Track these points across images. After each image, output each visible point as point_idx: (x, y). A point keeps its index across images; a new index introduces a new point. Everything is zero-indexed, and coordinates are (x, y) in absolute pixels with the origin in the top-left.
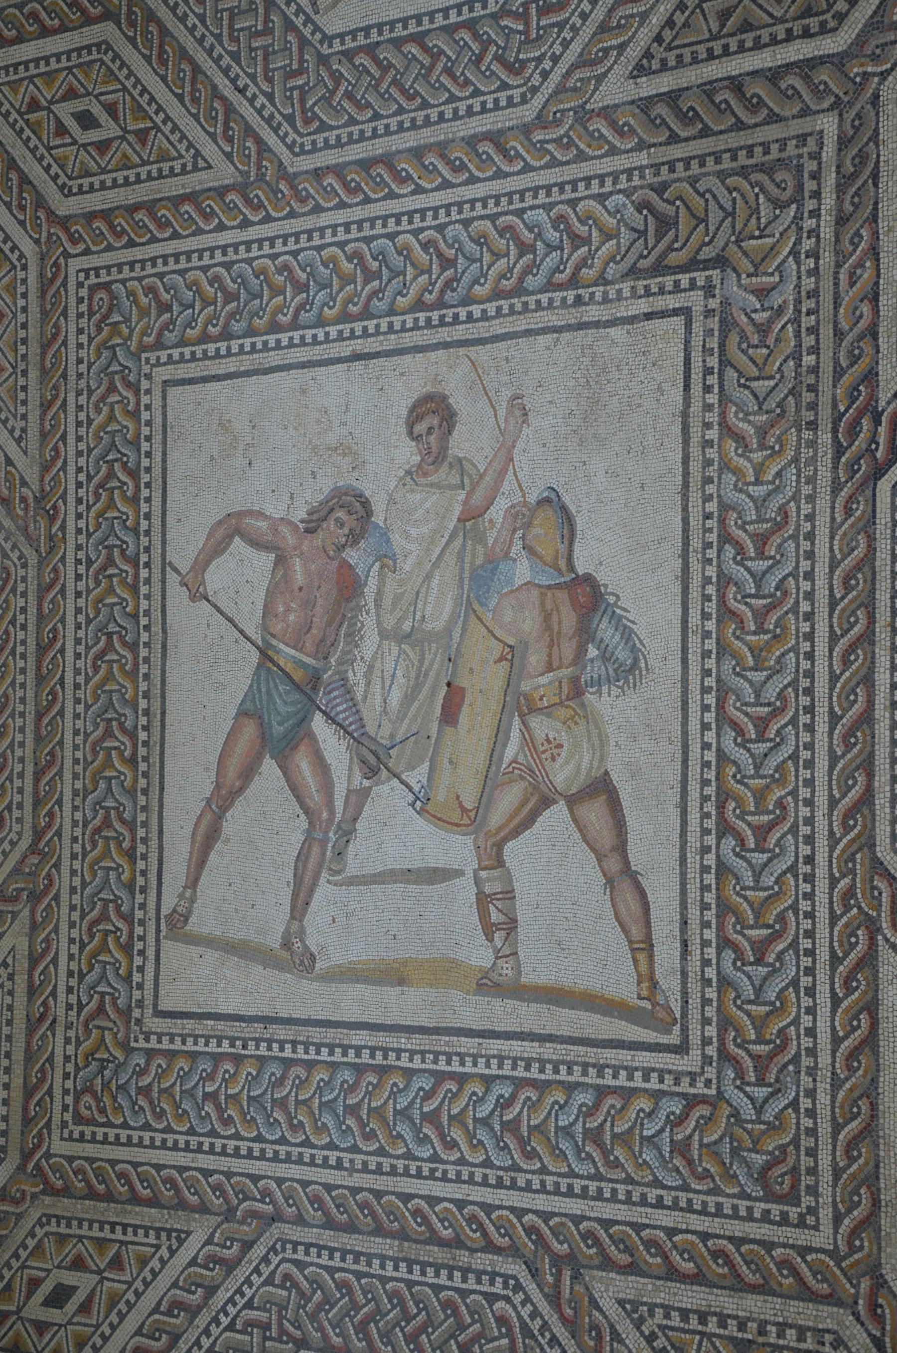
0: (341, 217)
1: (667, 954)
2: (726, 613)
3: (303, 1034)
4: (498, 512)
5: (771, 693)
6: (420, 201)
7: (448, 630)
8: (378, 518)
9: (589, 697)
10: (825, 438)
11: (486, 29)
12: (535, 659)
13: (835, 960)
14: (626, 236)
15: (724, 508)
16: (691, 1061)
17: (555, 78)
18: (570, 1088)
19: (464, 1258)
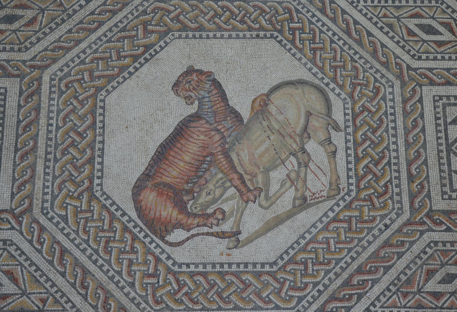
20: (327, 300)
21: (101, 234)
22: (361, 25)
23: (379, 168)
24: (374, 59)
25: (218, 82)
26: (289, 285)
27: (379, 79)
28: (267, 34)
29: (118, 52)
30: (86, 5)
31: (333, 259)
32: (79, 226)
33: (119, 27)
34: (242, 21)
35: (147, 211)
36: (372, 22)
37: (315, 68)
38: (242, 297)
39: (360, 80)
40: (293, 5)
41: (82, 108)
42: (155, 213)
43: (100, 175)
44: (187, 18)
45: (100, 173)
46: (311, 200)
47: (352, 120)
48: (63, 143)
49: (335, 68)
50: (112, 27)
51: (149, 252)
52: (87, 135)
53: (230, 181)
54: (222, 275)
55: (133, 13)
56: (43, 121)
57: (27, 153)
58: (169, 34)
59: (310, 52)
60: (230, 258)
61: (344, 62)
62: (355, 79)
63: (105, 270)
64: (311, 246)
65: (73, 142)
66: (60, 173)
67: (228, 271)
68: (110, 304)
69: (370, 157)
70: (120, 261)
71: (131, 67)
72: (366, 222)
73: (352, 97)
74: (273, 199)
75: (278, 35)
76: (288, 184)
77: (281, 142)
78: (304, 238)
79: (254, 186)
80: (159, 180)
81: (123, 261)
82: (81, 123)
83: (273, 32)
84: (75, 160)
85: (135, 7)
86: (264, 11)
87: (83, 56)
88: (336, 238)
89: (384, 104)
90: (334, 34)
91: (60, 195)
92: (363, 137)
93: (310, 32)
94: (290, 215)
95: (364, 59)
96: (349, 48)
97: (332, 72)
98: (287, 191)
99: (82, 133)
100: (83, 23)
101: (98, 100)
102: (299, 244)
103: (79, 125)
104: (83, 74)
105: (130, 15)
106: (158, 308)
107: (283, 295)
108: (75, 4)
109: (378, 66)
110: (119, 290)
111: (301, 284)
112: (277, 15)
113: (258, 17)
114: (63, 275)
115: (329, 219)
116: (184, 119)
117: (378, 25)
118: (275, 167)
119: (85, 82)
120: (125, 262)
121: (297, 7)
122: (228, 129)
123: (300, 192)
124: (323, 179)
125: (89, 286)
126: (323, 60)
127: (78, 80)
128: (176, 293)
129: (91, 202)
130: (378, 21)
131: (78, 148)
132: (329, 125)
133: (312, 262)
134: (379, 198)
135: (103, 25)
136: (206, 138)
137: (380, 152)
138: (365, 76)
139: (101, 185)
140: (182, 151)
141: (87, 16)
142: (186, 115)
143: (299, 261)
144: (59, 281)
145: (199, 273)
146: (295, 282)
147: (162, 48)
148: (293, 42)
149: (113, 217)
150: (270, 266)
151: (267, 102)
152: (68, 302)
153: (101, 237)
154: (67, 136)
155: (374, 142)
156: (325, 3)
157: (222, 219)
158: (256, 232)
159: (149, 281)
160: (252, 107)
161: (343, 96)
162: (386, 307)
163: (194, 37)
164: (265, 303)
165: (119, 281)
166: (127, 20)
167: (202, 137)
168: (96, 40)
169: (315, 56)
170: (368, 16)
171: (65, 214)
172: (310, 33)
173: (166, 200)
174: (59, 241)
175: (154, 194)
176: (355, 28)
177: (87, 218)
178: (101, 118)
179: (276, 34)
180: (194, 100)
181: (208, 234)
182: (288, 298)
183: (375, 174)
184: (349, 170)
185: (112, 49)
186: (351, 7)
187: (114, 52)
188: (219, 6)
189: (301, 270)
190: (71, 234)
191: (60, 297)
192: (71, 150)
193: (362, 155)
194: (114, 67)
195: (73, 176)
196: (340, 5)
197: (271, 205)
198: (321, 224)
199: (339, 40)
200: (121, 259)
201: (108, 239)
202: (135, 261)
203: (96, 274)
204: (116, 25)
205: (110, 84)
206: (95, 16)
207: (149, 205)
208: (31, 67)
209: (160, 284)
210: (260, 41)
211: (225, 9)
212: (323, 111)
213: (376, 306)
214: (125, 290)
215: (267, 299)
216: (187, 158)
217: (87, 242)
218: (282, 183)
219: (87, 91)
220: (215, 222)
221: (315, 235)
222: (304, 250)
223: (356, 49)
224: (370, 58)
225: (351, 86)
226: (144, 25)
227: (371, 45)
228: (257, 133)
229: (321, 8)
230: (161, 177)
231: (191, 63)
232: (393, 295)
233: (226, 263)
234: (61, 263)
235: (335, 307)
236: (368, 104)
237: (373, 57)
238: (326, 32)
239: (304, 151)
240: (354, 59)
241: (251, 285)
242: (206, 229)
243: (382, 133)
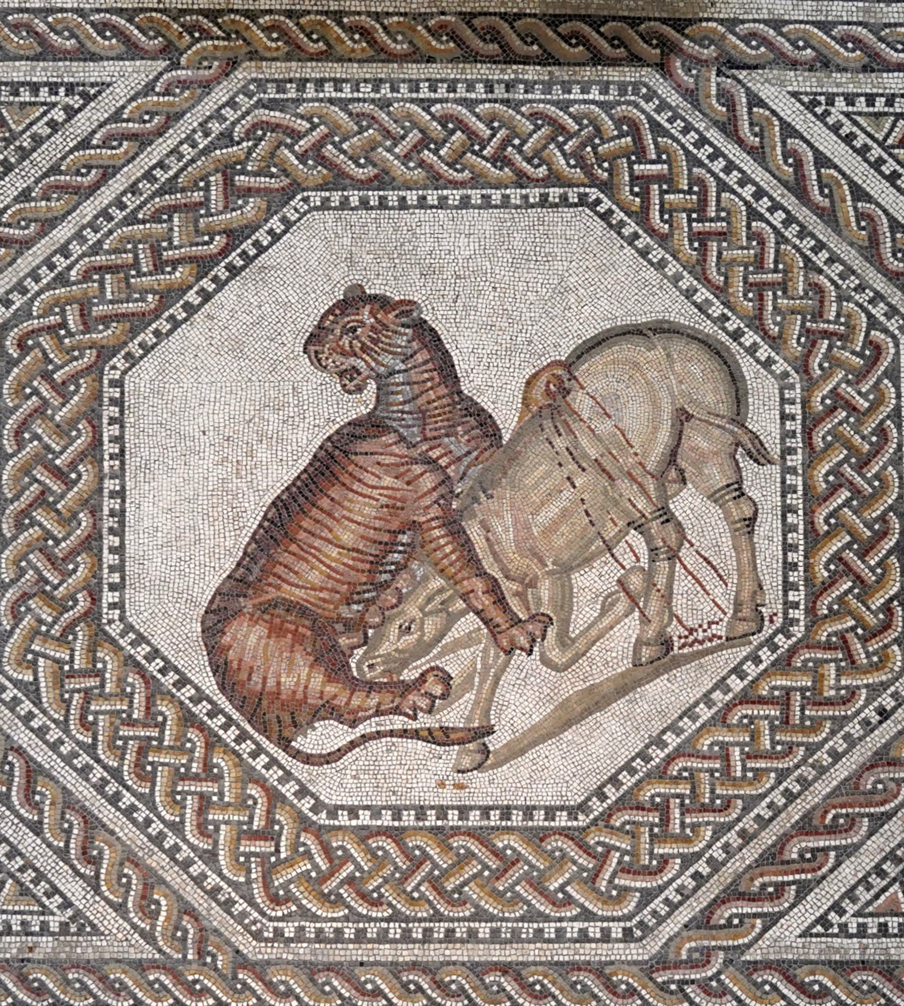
20: (717, 897)
21: (124, 732)
22: (836, 167)
23: (872, 563)
24: (871, 263)
25: (432, 330)
26: (619, 863)
27: (882, 319)
28: (570, 194)
29: (156, 251)
30: (66, 121)
31: (737, 797)
32: (68, 711)
33: (156, 180)
34: (500, 160)
35: (244, 676)
36: (866, 160)
37: (704, 290)
38: (495, 890)
39: (829, 322)
40: (643, 111)
41: (63, 405)
42: (265, 679)
43: (118, 580)
44: (345, 152)
45: (117, 575)
46: (684, 646)
47: (803, 431)
48: (17, 497)
49: (760, 289)
50: (138, 180)
51: (250, 776)
52: (80, 476)
53: (465, 597)
54: (441, 835)
55: (194, 140)
58: (294, 197)
59: (691, 244)
60: (463, 793)
61: (785, 272)
62: (813, 320)
63: (141, 819)
64: (680, 763)
65: (43, 493)
66: (13, 576)
67: (458, 828)
68: (158, 903)
69: (849, 533)
70: (178, 797)
71: (192, 292)
72: (829, 702)
73: (804, 368)
74: (580, 645)
75: (602, 196)
76: (622, 605)
77: (605, 493)
78: (660, 743)
79: (528, 609)
80: (272, 593)
81: (185, 799)
82: (62, 443)
83: (587, 190)
84: (50, 542)
85: (200, 124)
86: (562, 129)
87: (61, 262)
88: (746, 744)
89: (893, 390)
90: (759, 194)
91: (18, 631)
92: (831, 478)
93: (690, 188)
94: (624, 687)
95: (843, 263)
96: (800, 232)
97: (750, 300)
98: (618, 622)
99: (65, 469)
100: (61, 173)
101: (106, 382)
102: (647, 759)
103: (58, 449)
104: (63, 311)
105: (185, 146)
106: (280, 914)
107: (603, 885)
108: (39, 119)
109: (880, 284)
110: (176, 868)
111: (651, 859)
112: (597, 141)
113: (545, 147)
114: (36, 828)
115: (731, 695)
116: (337, 432)
117: (883, 168)
118: (588, 561)
119: (70, 334)
120: (189, 802)
121: (656, 116)
122: (459, 459)
123: (654, 626)
124: (719, 591)
125: (101, 858)
127: (51, 329)
128: (324, 878)
129: (95, 651)
130: (885, 156)
131: (57, 511)
132: (737, 445)
133: (682, 805)
134: (866, 641)
135: (114, 175)
136: (398, 484)
137: (876, 520)
138: (844, 312)
139: (119, 605)
140: (334, 519)
141: (71, 151)
142: (341, 421)
143: (647, 804)
144: (28, 842)
146: (634, 853)
147: (276, 238)
150: (569, 814)
151: (567, 385)
152: (53, 895)
153: (126, 739)
154: (27, 479)
155: (859, 492)
156: (734, 105)
157: (443, 697)
158: (533, 728)
159: (253, 849)
160: (524, 399)
161: (780, 366)
162: (871, 915)
163: (365, 204)
164: (554, 904)
165: (176, 848)
166: (179, 160)
167: (388, 481)
168: (96, 217)
169: (705, 255)
170: (858, 144)
171: (31, 679)
172: (690, 192)
173: (293, 646)
174: (20, 747)
175: (260, 630)
176: (819, 176)
177: (87, 691)
178: (115, 430)
179: (594, 193)
180: (364, 380)
181: (404, 733)
182: (614, 893)
183: (858, 577)
184: (789, 567)
185: (140, 242)
186: (809, 115)
187: (144, 250)
188: (433, 117)
189: (652, 826)
190: (49, 729)
191: (32, 881)
192: (39, 515)
193: (826, 528)
194: (147, 292)
195: (47, 582)
196: (778, 110)
197: (574, 660)
198: (710, 708)
199: (771, 210)
200: (179, 793)
201: (144, 744)
202: (215, 798)
203: (117, 830)
204: (149, 176)
205: (134, 337)
206: (93, 152)
207: (247, 658)
209: (283, 856)
211: (450, 126)
212: (723, 409)
213: (845, 912)
214: (194, 870)
215: (560, 895)
216: (346, 538)
217: (91, 749)
218: (604, 602)
219: (76, 359)
220: (423, 703)
221: (692, 736)
222: (660, 774)
223: (821, 237)
225: (803, 340)
226: (224, 174)
227: (863, 224)
228: (538, 470)
229: (725, 119)
230: (278, 588)
231: (356, 277)
232: (890, 885)
233: (453, 808)
234: (28, 800)
235: (736, 915)
236: (849, 389)
237: (866, 259)
238: (735, 187)
239: (666, 516)
240: (814, 263)
241: (518, 861)
242: (398, 722)
243: (884, 468)
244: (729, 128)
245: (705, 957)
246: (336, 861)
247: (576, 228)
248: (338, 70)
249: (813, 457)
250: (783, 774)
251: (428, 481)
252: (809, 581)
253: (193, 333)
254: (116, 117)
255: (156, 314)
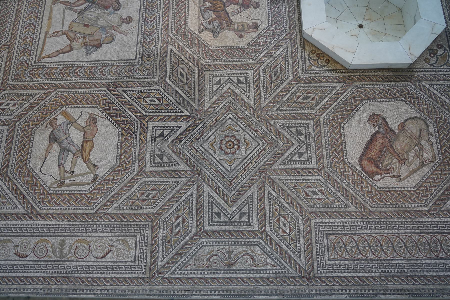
0: (162, 4)
1: (48, 60)
2: (92, 67)
3: (44, 4)
4: (114, 32)
5: (81, 74)
6: (161, 17)
7: (98, 24)
8: (116, 12)
9: (84, 47)
10: (114, 81)
11: (184, 26)
12: (91, 39)
13: (44, 84)
14: (148, 50)
15: (107, 66)
16: (33, 64)
17: (174, 38)
18: (32, 46)
19: (11, 31)
29: (346, 109)
49: (428, 112)
54: (396, 192)
56: (323, 136)
57: (319, 147)
73: (436, 123)
76: (416, 157)
94: (418, 169)
109: (445, 111)
114: (339, 191)
118: (410, 151)
126: (423, 109)
128: (380, 198)
143: (424, 186)
145: (388, 191)
148: (411, 102)
149: (353, 171)
161: (433, 123)
181: (388, 177)
184: (439, 151)
208: (316, 115)
210: (398, 102)
217: (345, 180)
222: (425, 182)
224: (441, 108)
228: (402, 138)
239: (421, 145)
242: (388, 175)
244: (421, 89)
245: (436, 210)
246: (382, 196)
247: (402, 104)
248: (367, 83)
249: (440, 135)
250: (443, 182)
251: (387, 140)
252: (442, 153)
253: (352, 120)
254: (338, 91)
255: (347, 117)
